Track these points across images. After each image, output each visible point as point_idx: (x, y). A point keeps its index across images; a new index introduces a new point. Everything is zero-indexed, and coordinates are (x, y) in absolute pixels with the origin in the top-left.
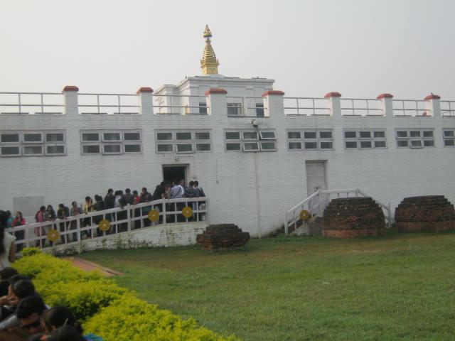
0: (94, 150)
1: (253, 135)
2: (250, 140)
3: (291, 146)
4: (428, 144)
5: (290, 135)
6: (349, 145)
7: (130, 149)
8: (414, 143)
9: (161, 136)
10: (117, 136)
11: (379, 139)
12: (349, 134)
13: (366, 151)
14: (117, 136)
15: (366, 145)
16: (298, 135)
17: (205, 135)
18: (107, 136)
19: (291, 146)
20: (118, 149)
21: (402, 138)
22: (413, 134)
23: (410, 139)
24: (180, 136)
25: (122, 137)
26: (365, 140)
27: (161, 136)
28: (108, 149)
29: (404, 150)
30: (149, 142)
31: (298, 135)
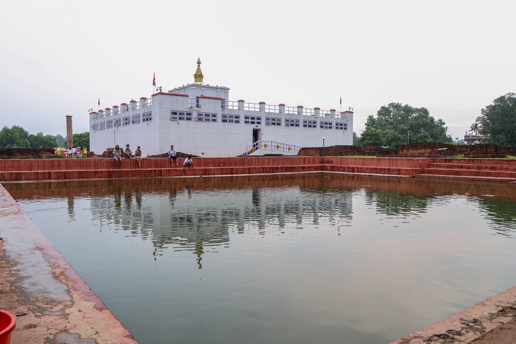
0: (226, 121)
1: (274, 120)
2: (273, 122)
6: (305, 126)
7: (236, 122)
9: (246, 118)
11: (315, 125)
13: (310, 128)
14: (232, 117)
15: (310, 126)
16: (288, 121)
18: (229, 117)
25: (234, 117)
29: (322, 129)
30: (242, 120)
31: (288, 121)
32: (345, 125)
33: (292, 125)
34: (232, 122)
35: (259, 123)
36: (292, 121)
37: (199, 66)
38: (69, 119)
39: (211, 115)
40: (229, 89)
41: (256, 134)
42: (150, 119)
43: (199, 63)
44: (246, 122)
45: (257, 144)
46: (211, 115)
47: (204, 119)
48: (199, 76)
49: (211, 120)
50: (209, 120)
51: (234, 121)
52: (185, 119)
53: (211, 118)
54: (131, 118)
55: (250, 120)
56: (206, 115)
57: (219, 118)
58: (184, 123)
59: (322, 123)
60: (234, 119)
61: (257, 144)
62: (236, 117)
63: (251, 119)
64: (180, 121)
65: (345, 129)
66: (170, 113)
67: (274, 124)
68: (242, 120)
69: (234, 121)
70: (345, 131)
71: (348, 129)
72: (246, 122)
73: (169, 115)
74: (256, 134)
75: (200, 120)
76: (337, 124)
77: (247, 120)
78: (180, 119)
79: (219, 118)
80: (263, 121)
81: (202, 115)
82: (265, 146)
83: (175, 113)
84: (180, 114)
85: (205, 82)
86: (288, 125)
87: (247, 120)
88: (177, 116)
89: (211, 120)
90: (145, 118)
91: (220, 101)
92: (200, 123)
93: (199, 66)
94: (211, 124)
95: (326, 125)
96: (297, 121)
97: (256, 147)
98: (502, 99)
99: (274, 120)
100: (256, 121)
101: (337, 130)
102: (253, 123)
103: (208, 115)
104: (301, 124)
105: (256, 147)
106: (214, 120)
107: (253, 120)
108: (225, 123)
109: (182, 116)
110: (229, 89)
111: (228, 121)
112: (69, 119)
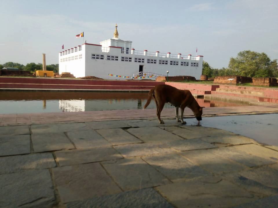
2: (152, 61)
3: (160, 63)
4: (187, 65)
5: (160, 61)
7: (130, 61)
8: (184, 65)
10: (128, 58)
12: (171, 62)
13: (174, 66)
14: (128, 58)
17: (143, 59)
18: (126, 58)
19: (160, 63)
20: (127, 61)
21: (182, 64)
22: (185, 63)
23: (183, 64)
24: (139, 59)
25: (128, 58)
26: (174, 63)
27: (136, 59)
28: (126, 61)
29: (182, 66)
30: (133, 60)
31: (161, 61)
32: (197, 64)
33: (163, 63)
34: (127, 61)
35: (143, 62)
36: (163, 61)
37: (116, 28)
38: (44, 55)
39: (115, 57)
40: (131, 42)
41: (141, 68)
42: (82, 58)
43: (117, 27)
45: (140, 74)
46: (115, 57)
47: (111, 59)
48: (117, 34)
49: (115, 60)
50: (113, 59)
51: (128, 61)
52: (100, 58)
53: (115, 58)
54: (75, 56)
55: (138, 60)
56: (112, 57)
57: (120, 59)
58: (99, 60)
59: (182, 63)
60: (128, 60)
61: (140, 74)
63: (139, 60)
64: (97, 60)
65: (197, 66)
66: (91, 55)
67: (152, 63)
68: (133, 60)
69: (128, 61)
70: (197, 67)
71: (199, 66)
72: (135, 61)
73: (91, 56)
74: (141, 68)
75: (109, 59)
76: (192, 63)
77: (136, 60)
78: (97, 58)
79: (120, 59)
80: (146, 61)
81: (109, 57)
82: (145, 75)
83: (94, 55)
84: (97, 55)
85: (120, 37)
86: (161, 63)
87: (136, 60)
88: (96, 57)
89: (115, 60)
90: (80, 57)
91: (121, 49)
92: (109, 61)
93: (116, 28)
94: (115, 61)
95: (185, 64)
96: (166, 61)
97: (141, 75)
98: (32, 63)
99: (152, 60)
100: (141, 61)
101: (192, 67)
102: (139, 62)
103: (113, 57)
104: (169, 63)
105: (141, 75)
106: (117, 60)
107: (139, 60)
108: (123, 61)
110: (131, 42)
111: (125, 60)
112: (44, 55)
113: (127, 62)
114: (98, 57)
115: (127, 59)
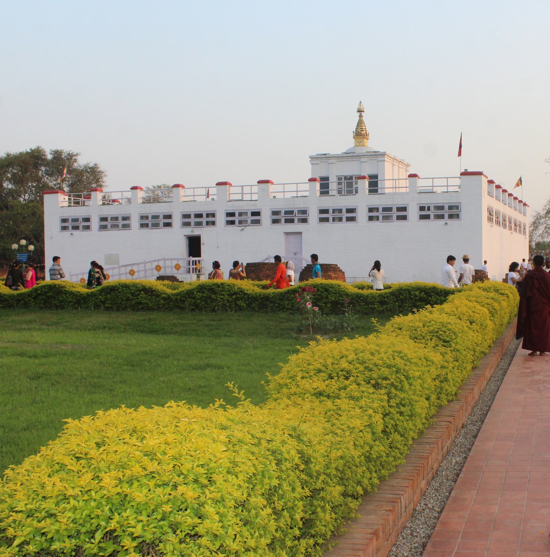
9: (371, 210)
14: (340, 211)
18: (334, 211)
24: (385, 209)
25: (344, 211)
30: (362, 214)
34: (340, 219)
44: (371, 218)
60: (345, 215)
62: (349, 211)
69: (344, 219)
72: (371, 218)
77: (374, 214)
87: (374, 214)
108: (325, 224)
109: (243, 218)
111: (331, 219)
113: (338, 225)
114: (242, 218)
115: (337, 215)
